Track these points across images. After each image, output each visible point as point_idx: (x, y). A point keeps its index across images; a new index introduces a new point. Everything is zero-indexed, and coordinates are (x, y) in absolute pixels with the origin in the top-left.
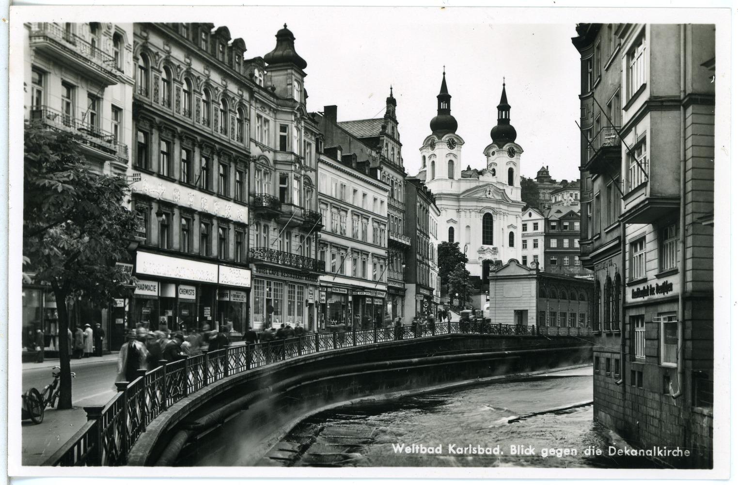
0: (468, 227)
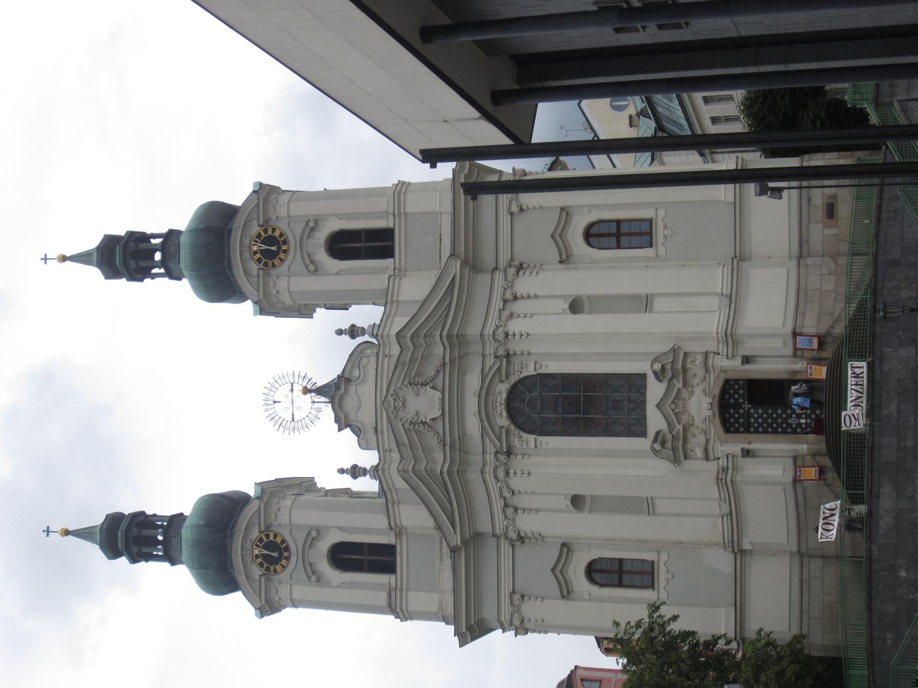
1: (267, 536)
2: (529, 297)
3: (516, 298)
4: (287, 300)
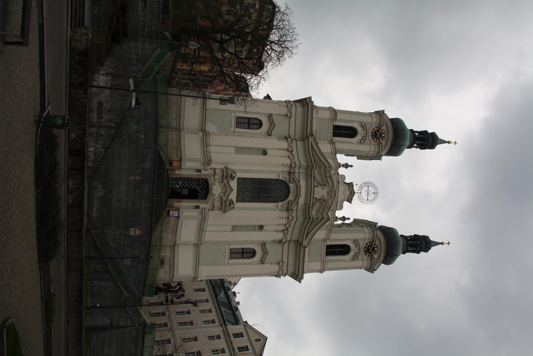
0: (265, 153)
1: (379, 141)
2: (278, 231)
3: (283, 231)
4: (367, 230)
